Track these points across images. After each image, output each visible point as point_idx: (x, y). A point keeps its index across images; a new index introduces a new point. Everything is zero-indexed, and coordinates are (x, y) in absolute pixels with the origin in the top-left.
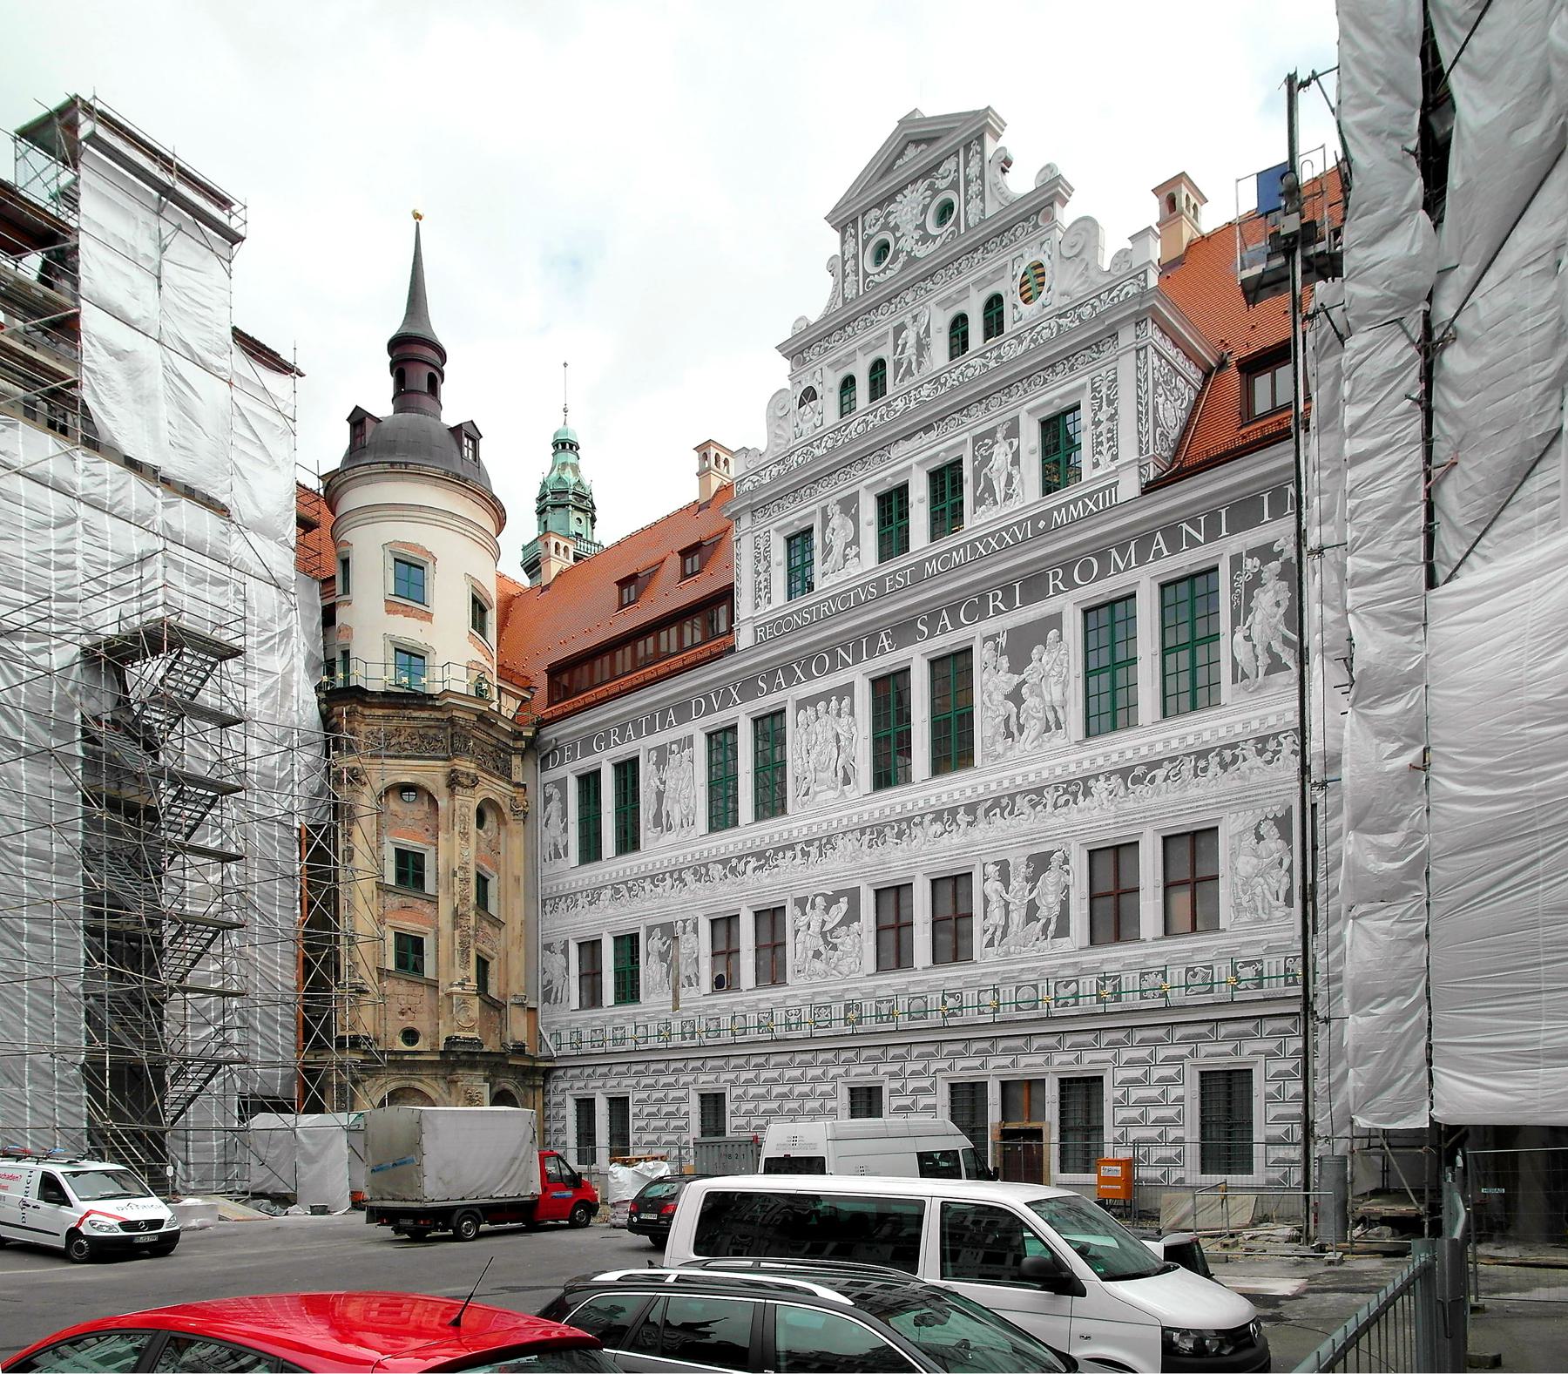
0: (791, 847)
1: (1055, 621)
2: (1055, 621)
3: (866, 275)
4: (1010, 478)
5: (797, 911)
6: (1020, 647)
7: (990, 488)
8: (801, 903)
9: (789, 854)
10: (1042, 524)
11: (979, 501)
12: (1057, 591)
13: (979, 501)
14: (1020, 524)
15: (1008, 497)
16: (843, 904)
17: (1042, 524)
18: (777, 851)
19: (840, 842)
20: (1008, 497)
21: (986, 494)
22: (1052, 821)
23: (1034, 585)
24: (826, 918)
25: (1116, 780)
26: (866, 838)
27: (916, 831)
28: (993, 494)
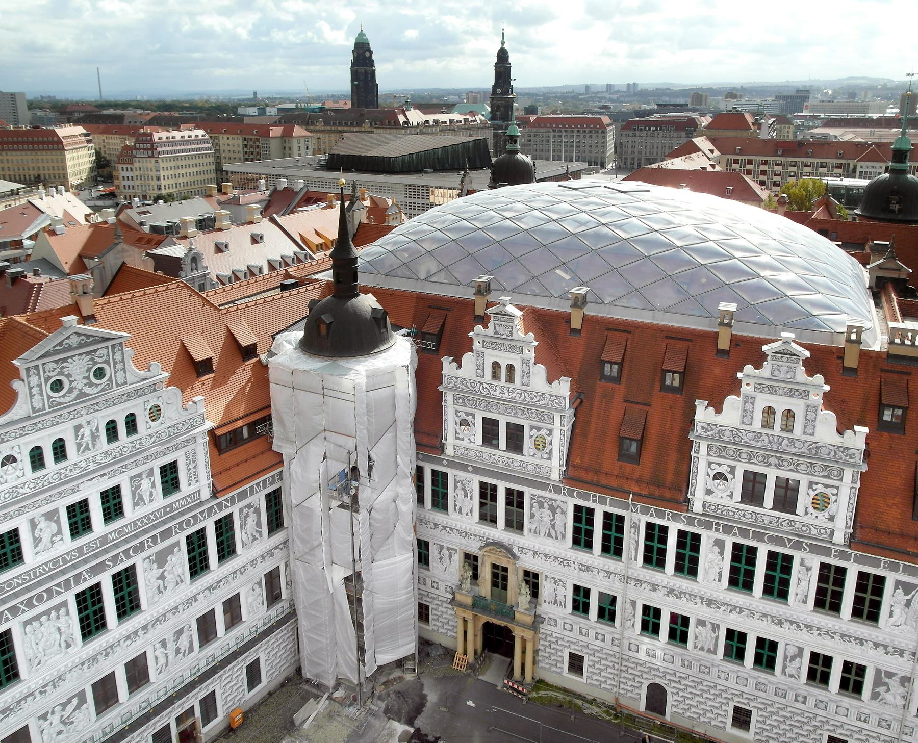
0: (32, 694)
1: (177, 544)
2: (177, 544)
3: (49, 397)
4: (151, 493)
5: (42, 721)
6: (161, 559)
7: (141, 498)
8: (44, 717)
9: (31, 697)
10: (168, 510)
11: (136, 504)
12: (177, 533)
13: (136, 504)
14: (158, 511)
15: (151, 501)
16: (75, 701)
17: (168, 510)
18: (19, 702)
19: (68, 676)
20: (151, 501)
21: (138, 501)
22: (183, 616)
23: (166, 534)
24: (63, 713)
25: (207, 592)
26: (86, 666)
27: (118, 649)
28: (143, 500)
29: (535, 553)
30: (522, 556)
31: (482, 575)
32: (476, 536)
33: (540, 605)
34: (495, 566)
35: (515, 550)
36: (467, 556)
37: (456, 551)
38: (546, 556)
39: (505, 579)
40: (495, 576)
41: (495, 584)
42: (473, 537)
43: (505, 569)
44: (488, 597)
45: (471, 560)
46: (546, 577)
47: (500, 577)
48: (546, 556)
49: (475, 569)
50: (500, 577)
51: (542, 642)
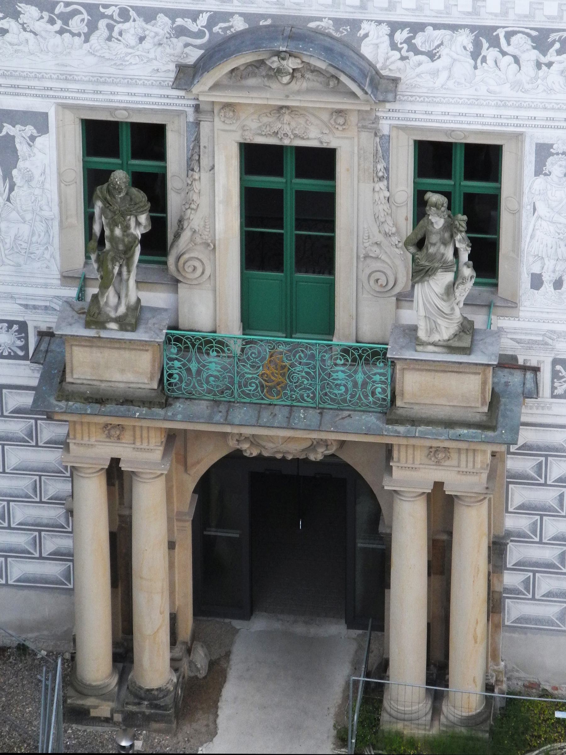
29: (485, 37)
30: (414, 73)
31: (195, 220)
32: (149, 15)
33: (512, 305)
34: (257, 158)
35: (375, 47)
36: (100, 136)
37: (40, 122)
38: (541, 40)
39: (320, 212)
40: (258, 208)
41: (259, 252)
42: (132, 28)
43: (320, 162)
44: (231, 325)
45: (123, 154)
46: (544, 151)
47: (289, 210)
48: (541, 40)
49: (153, 187)
50: (289, 210)
51: (519, 495)
